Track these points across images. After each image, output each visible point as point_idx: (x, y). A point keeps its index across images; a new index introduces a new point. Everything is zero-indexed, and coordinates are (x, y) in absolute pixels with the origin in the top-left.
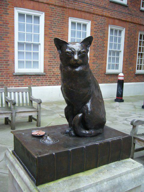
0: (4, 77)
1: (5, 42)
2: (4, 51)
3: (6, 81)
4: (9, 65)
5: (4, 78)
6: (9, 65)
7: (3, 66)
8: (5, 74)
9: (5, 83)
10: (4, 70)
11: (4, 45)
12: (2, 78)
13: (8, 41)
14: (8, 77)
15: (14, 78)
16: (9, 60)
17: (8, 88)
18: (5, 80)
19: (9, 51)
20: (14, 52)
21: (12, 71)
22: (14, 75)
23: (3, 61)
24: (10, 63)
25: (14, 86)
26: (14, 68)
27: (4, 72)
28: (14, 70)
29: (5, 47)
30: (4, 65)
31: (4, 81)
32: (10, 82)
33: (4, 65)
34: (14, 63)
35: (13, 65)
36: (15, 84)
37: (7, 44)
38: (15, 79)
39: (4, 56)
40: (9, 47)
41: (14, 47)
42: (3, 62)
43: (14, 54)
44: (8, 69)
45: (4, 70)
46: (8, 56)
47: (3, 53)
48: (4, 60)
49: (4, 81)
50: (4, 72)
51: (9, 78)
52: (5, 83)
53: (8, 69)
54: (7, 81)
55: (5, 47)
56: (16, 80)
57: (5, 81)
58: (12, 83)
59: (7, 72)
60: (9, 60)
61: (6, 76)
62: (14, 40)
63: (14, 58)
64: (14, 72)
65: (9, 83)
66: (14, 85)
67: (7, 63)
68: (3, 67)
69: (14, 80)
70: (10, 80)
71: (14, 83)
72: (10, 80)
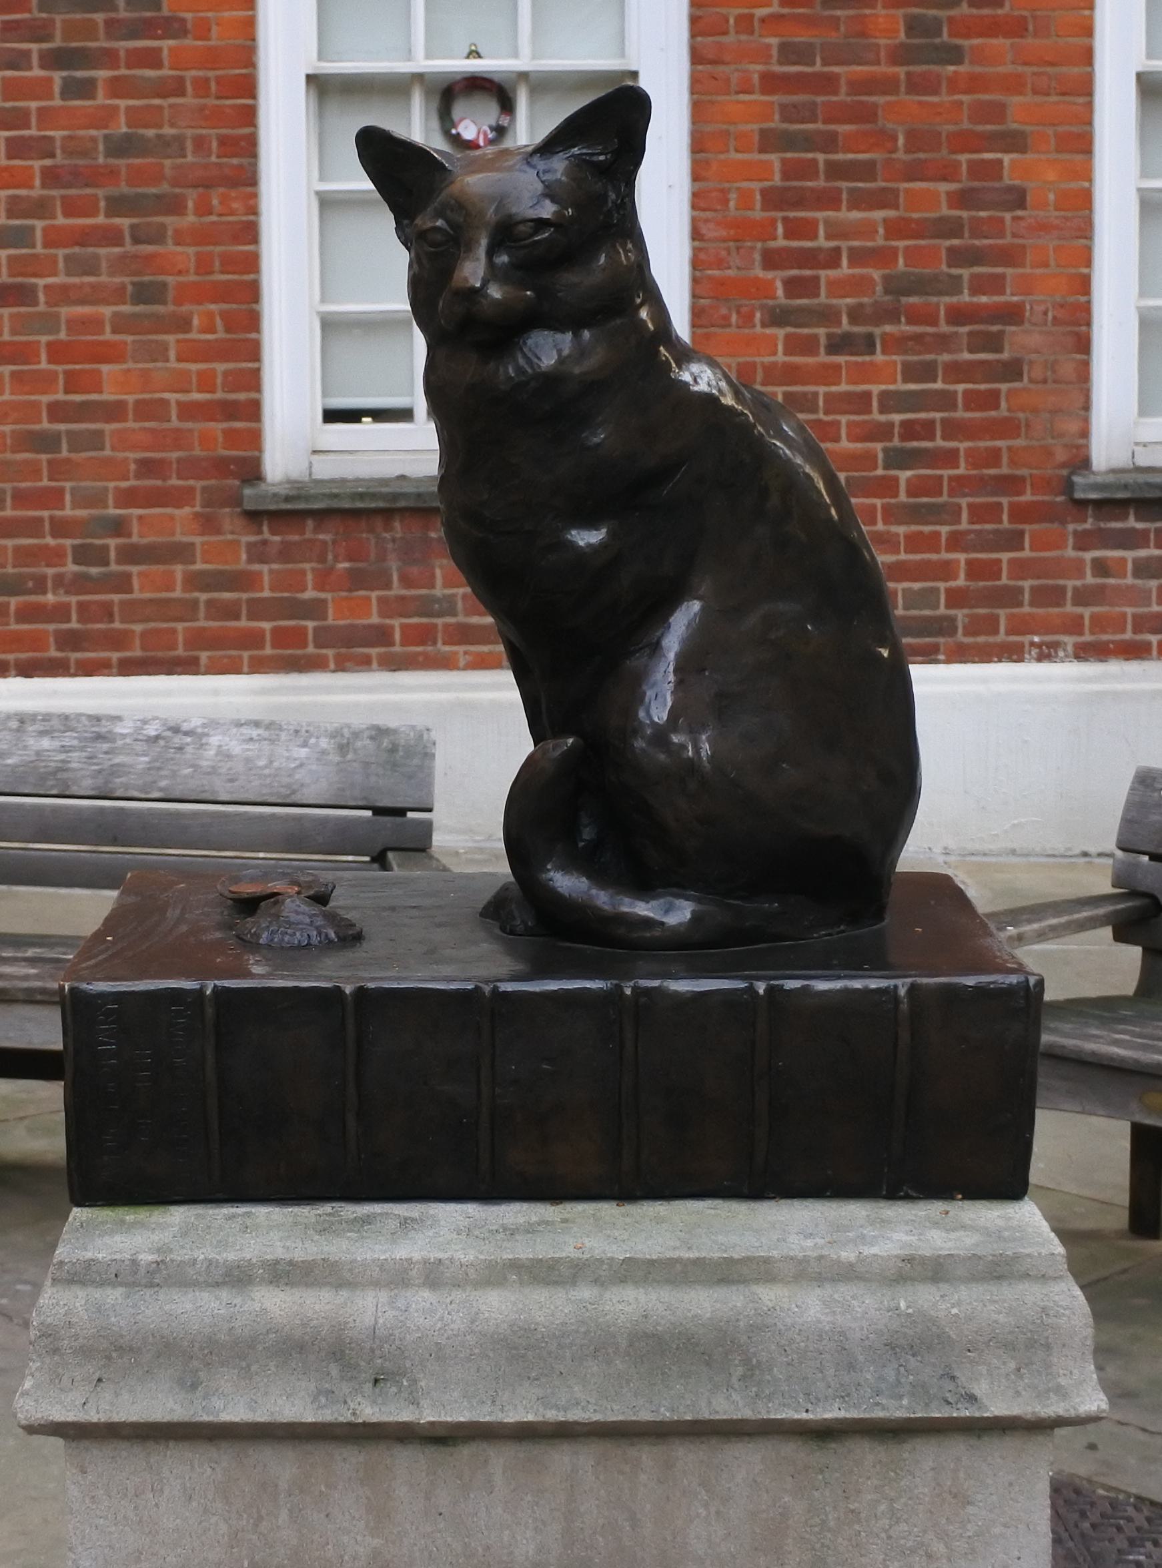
0: (944, 530)
1: (975, 83)
2: (962, 199)
3: (976, 570)
4: (1013, 370)
5: (956, 542)
6: (1013, 370)
7: (939, 385)
8: (959, 485)
9: (956, 598)
10: (953, 429)
11: (966, 125)
12: (931, 543)
13: (1008, 69)
14: (1006, 524)
15: (1084, 542)
16: (1013, 314)
17: (905, 640)
18: (962, 557)
19: (1018, 198)
20: (1080, 205)
21: (1048, 452)
22: (1083, 504)
23: (944, 328)
24: (1022, 341)
25: (1069, 640)
26: (1087, 407)
27: (950, 458)
28: (1085, 433)
29: (964, 142)
30: (958, 371)
31: (945, 571)
32: (1027, 584)
33: (958, 371)
34: (1083, 345)
35: (1067, 369)
36: (1087, 612)
37: (997, 112)
38: (1089, 556)
39: (958, 257)
40: (1015, 142)
41: (1080, 142)
42: (944, 342)
43: (1086, 230)
44: (1008, 428)
45: (953, 429)
46: (1009, 256)
47: (952, 228)
48: (958, 316)
49: (945, 571)
50: (950, 458)
51: (1013, 541)
52: (956, 598)
53: (1008, 428)
54: (992, 571)
55: (964, 142)
56: (1101, 568)
57: (961, 582)
58: (1053, 596)
59: (993, 457)
60: (1013, 314)
61: (978, 514)
62: (1087, 56)
63: (1084, 285)
64: (1083, 463)
65: (1011, 597)
66: (1074, 626)
67: (994, 343)
68: (945, 401)
69: (1077, 569)
70: (1021, 569)
71: (1082, 597)
72: (1021, 569)
